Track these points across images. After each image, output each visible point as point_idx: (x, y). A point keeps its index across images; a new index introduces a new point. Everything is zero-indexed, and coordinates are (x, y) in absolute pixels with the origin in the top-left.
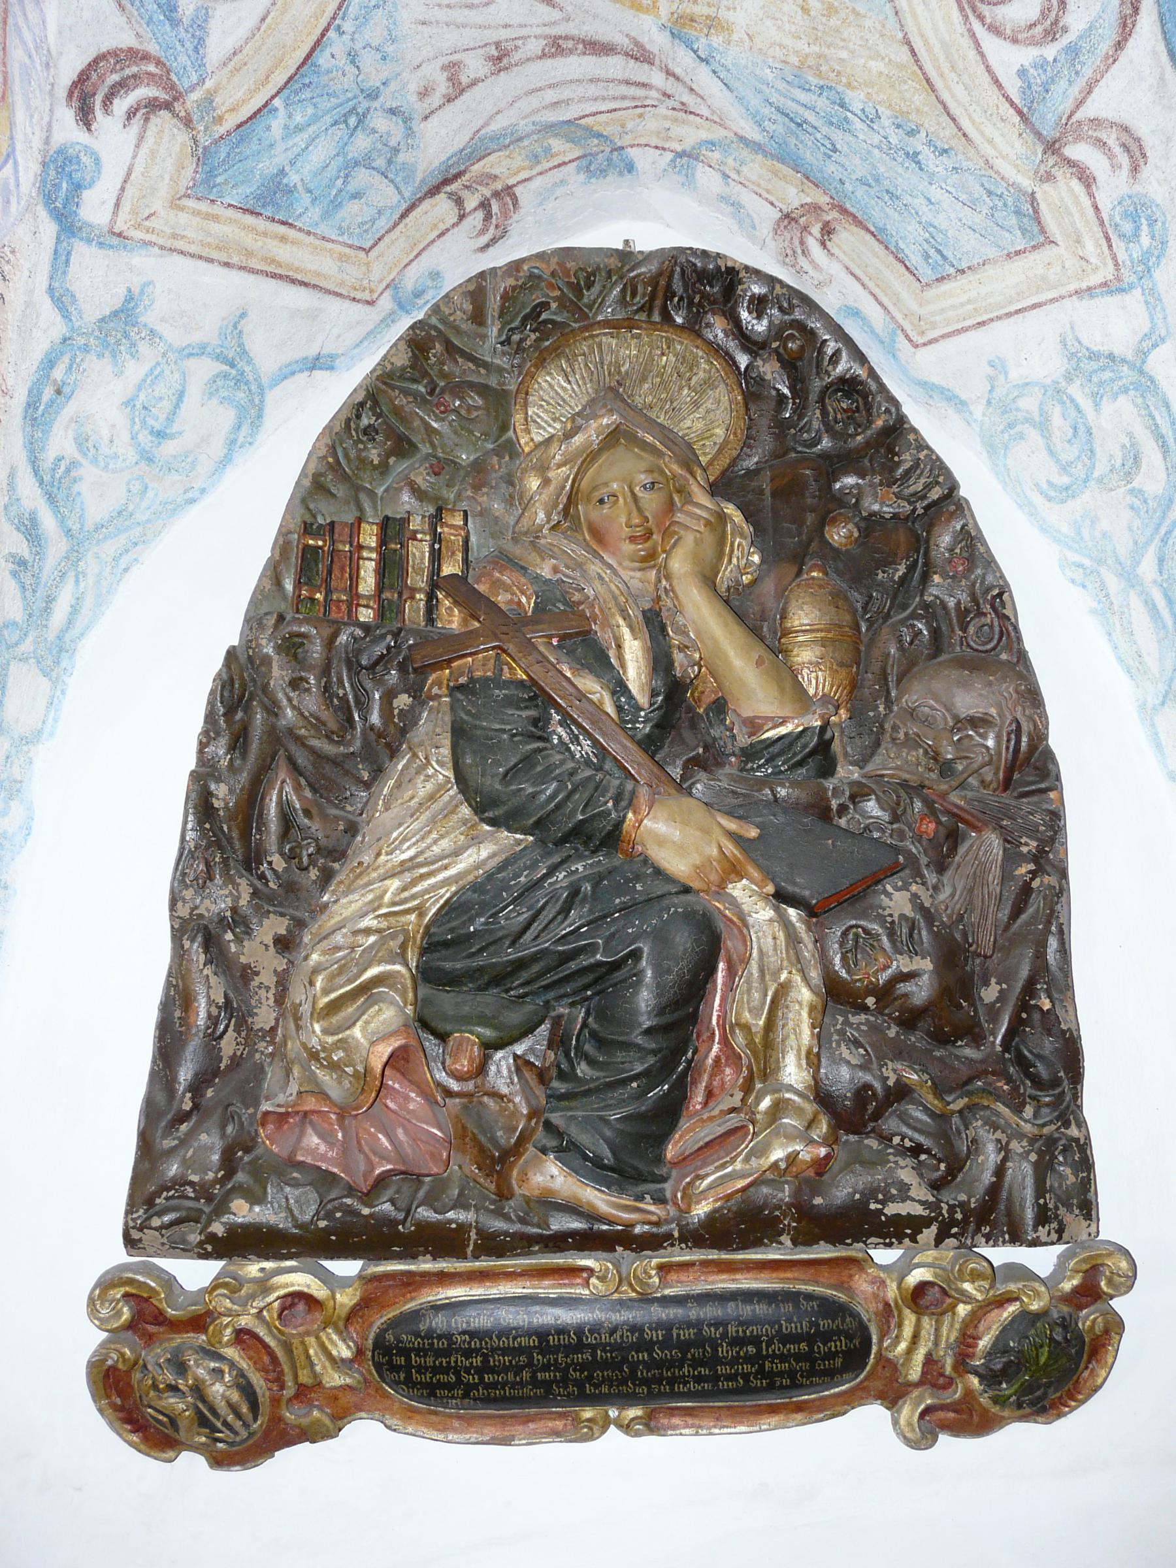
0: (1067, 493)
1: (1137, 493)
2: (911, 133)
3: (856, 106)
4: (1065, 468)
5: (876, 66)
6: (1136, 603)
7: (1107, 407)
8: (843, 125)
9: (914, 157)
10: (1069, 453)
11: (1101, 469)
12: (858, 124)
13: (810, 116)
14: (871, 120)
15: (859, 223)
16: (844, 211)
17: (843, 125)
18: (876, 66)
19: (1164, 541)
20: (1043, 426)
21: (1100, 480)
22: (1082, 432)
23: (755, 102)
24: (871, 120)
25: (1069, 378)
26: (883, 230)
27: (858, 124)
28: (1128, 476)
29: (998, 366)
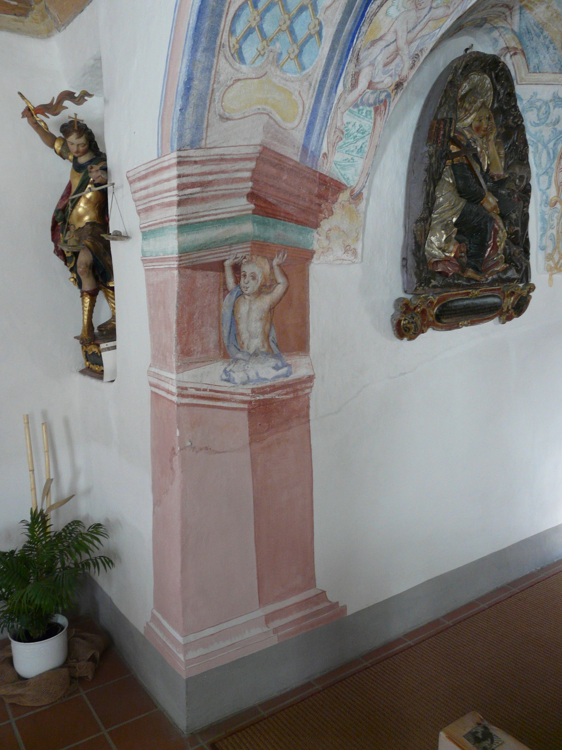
0: (537, 125)
1: (555, 129)
2: (551, 43)
3: (544, 34)
4: (539, 120)
5: (555, 29)
6: (545, 152)
7: (556, 109)
8: (539, 36)
9: (548, 48)
10: (542, 116)
11: (548, 121)
12: (542, 37)
13: (533, 32)
14: (545, 38)
15: (524, 55)
16: (523, 51)
17: (539, 36)
18: (555, 29)
19: (557, 140)
20: (539, 110)
21: (547, 124)
22: (548, 113)
23: (523, 24)
24: (545, 38)
25: (551, 101)
26: (529, 58)
27: (542, 37)
28: (555, 125)
29: (535, 94)
